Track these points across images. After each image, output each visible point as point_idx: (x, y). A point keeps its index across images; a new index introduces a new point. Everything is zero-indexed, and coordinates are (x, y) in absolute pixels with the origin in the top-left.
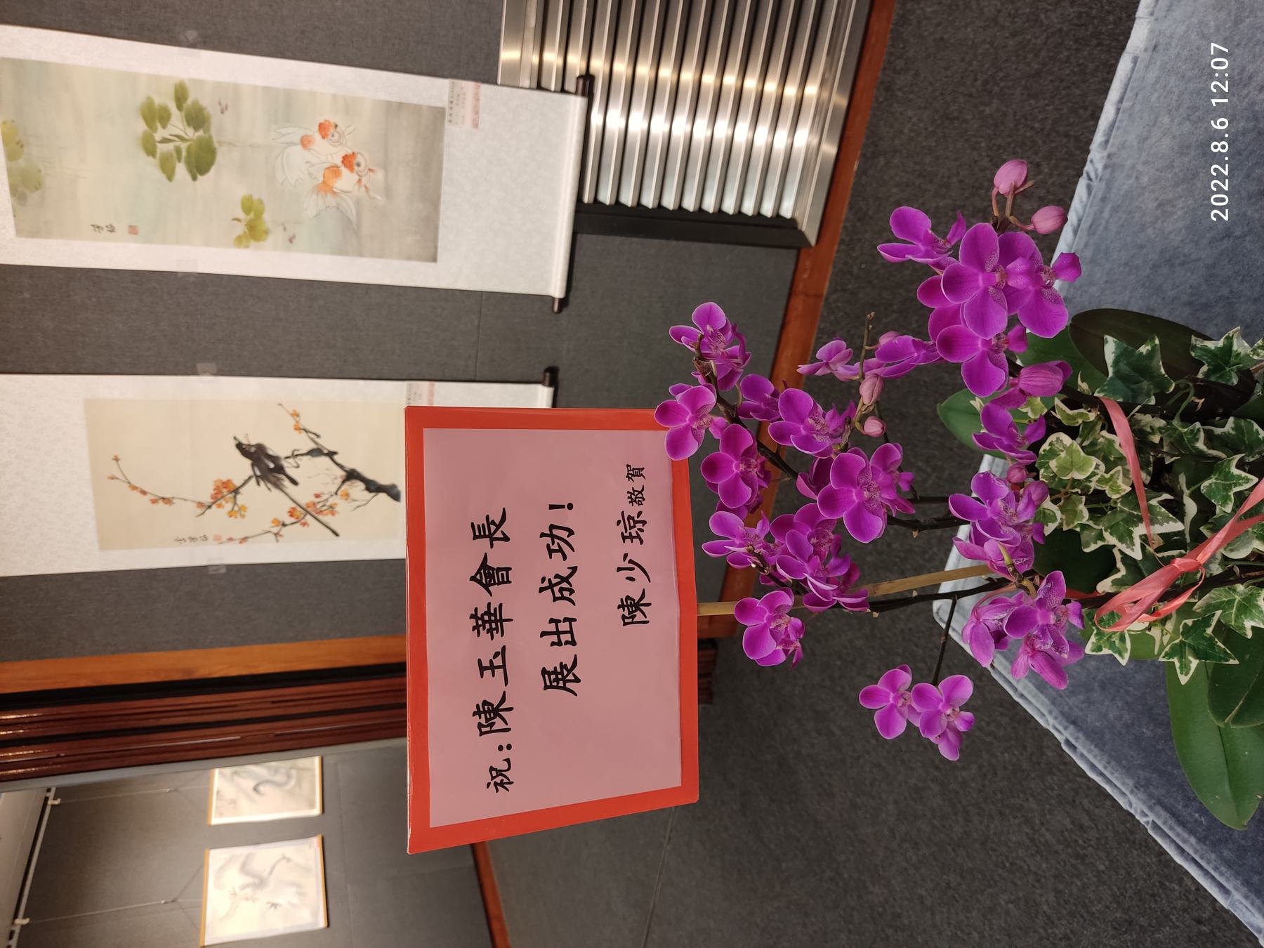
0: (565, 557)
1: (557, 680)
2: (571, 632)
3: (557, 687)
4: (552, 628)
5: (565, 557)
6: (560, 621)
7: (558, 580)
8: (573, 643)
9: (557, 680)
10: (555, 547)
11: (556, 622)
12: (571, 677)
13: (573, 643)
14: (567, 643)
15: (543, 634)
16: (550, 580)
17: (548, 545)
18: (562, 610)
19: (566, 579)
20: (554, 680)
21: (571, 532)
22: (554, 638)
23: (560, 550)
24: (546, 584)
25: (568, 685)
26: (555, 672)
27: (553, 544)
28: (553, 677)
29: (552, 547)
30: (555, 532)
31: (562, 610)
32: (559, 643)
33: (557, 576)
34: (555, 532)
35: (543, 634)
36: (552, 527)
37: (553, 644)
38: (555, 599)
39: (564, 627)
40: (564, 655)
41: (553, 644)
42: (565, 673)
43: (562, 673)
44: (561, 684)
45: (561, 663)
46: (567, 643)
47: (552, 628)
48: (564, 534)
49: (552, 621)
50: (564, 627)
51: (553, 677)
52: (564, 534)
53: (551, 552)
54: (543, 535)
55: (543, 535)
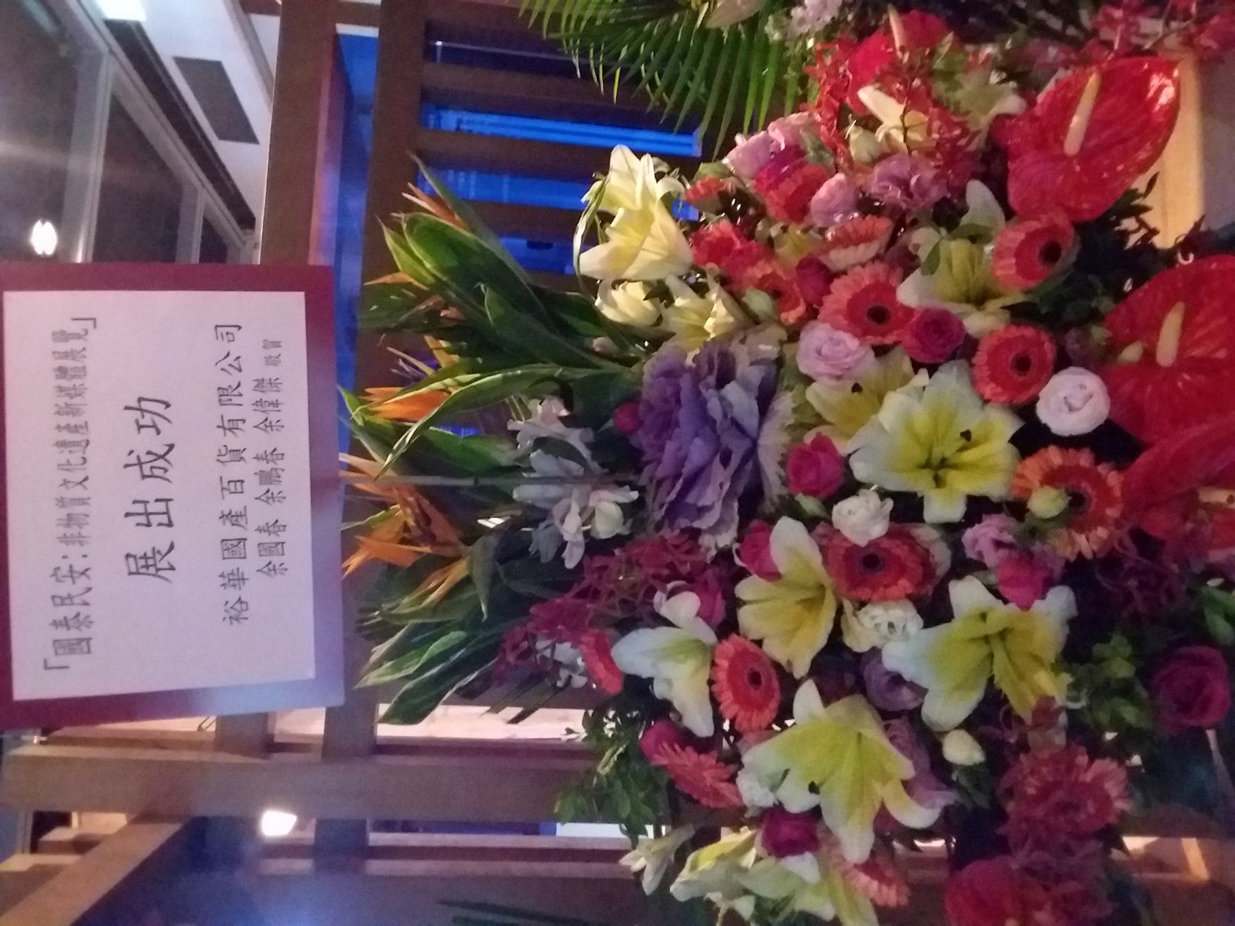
0: (158, 432)
1: (147, 567)
2: (167, 513)
3: (143, 574)
4: (139, 508)
5: (158, 432)
6: (148, 502)
7: (152, 457)
8: (170, 524)
9: (147, 567)
10: (147, 420)
11: (145, 502)
12: (163, 564)
13: (170, 524)
14: (160, 524)
15: (127, 515)
16: (138, 458)
17: (137, 422)
18: (153, 489)
19: (162, 457)
20: (143, 567)
21: (168, 405)
22: (143, 519)
23: (154, 426)
24: (133, 459)
25: (160, 573)
26: (145, 557)
27: (143, 417)
28: (142, 562)
29: (142, 422)
30: (144, 405)
31: (153, 489)
32: (149, 525)
33: (149, 453)
34: (144, 405)
35: (127, 515)
36: (140, 400)
37: (138, 524)
38: (144, 477)
39: (161, 507)
40: (157, 537)
41: (138, 524)
42: (158, 557)
43: (153, 558)
44: (152, 570)
45: (154, 549)
46: (160, 524)
47: (139, 508)
48: (159, 408)
49: (135, 502)
50: (152, 507)
51: (142, 562)
52: (159, 408)
53: (140, 427)
54: (127, 408)
55: (127, 408)
